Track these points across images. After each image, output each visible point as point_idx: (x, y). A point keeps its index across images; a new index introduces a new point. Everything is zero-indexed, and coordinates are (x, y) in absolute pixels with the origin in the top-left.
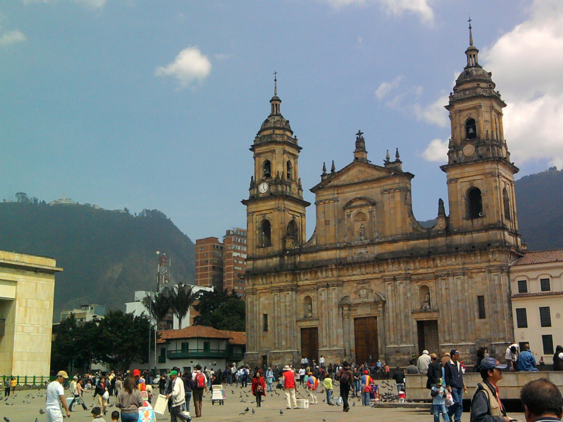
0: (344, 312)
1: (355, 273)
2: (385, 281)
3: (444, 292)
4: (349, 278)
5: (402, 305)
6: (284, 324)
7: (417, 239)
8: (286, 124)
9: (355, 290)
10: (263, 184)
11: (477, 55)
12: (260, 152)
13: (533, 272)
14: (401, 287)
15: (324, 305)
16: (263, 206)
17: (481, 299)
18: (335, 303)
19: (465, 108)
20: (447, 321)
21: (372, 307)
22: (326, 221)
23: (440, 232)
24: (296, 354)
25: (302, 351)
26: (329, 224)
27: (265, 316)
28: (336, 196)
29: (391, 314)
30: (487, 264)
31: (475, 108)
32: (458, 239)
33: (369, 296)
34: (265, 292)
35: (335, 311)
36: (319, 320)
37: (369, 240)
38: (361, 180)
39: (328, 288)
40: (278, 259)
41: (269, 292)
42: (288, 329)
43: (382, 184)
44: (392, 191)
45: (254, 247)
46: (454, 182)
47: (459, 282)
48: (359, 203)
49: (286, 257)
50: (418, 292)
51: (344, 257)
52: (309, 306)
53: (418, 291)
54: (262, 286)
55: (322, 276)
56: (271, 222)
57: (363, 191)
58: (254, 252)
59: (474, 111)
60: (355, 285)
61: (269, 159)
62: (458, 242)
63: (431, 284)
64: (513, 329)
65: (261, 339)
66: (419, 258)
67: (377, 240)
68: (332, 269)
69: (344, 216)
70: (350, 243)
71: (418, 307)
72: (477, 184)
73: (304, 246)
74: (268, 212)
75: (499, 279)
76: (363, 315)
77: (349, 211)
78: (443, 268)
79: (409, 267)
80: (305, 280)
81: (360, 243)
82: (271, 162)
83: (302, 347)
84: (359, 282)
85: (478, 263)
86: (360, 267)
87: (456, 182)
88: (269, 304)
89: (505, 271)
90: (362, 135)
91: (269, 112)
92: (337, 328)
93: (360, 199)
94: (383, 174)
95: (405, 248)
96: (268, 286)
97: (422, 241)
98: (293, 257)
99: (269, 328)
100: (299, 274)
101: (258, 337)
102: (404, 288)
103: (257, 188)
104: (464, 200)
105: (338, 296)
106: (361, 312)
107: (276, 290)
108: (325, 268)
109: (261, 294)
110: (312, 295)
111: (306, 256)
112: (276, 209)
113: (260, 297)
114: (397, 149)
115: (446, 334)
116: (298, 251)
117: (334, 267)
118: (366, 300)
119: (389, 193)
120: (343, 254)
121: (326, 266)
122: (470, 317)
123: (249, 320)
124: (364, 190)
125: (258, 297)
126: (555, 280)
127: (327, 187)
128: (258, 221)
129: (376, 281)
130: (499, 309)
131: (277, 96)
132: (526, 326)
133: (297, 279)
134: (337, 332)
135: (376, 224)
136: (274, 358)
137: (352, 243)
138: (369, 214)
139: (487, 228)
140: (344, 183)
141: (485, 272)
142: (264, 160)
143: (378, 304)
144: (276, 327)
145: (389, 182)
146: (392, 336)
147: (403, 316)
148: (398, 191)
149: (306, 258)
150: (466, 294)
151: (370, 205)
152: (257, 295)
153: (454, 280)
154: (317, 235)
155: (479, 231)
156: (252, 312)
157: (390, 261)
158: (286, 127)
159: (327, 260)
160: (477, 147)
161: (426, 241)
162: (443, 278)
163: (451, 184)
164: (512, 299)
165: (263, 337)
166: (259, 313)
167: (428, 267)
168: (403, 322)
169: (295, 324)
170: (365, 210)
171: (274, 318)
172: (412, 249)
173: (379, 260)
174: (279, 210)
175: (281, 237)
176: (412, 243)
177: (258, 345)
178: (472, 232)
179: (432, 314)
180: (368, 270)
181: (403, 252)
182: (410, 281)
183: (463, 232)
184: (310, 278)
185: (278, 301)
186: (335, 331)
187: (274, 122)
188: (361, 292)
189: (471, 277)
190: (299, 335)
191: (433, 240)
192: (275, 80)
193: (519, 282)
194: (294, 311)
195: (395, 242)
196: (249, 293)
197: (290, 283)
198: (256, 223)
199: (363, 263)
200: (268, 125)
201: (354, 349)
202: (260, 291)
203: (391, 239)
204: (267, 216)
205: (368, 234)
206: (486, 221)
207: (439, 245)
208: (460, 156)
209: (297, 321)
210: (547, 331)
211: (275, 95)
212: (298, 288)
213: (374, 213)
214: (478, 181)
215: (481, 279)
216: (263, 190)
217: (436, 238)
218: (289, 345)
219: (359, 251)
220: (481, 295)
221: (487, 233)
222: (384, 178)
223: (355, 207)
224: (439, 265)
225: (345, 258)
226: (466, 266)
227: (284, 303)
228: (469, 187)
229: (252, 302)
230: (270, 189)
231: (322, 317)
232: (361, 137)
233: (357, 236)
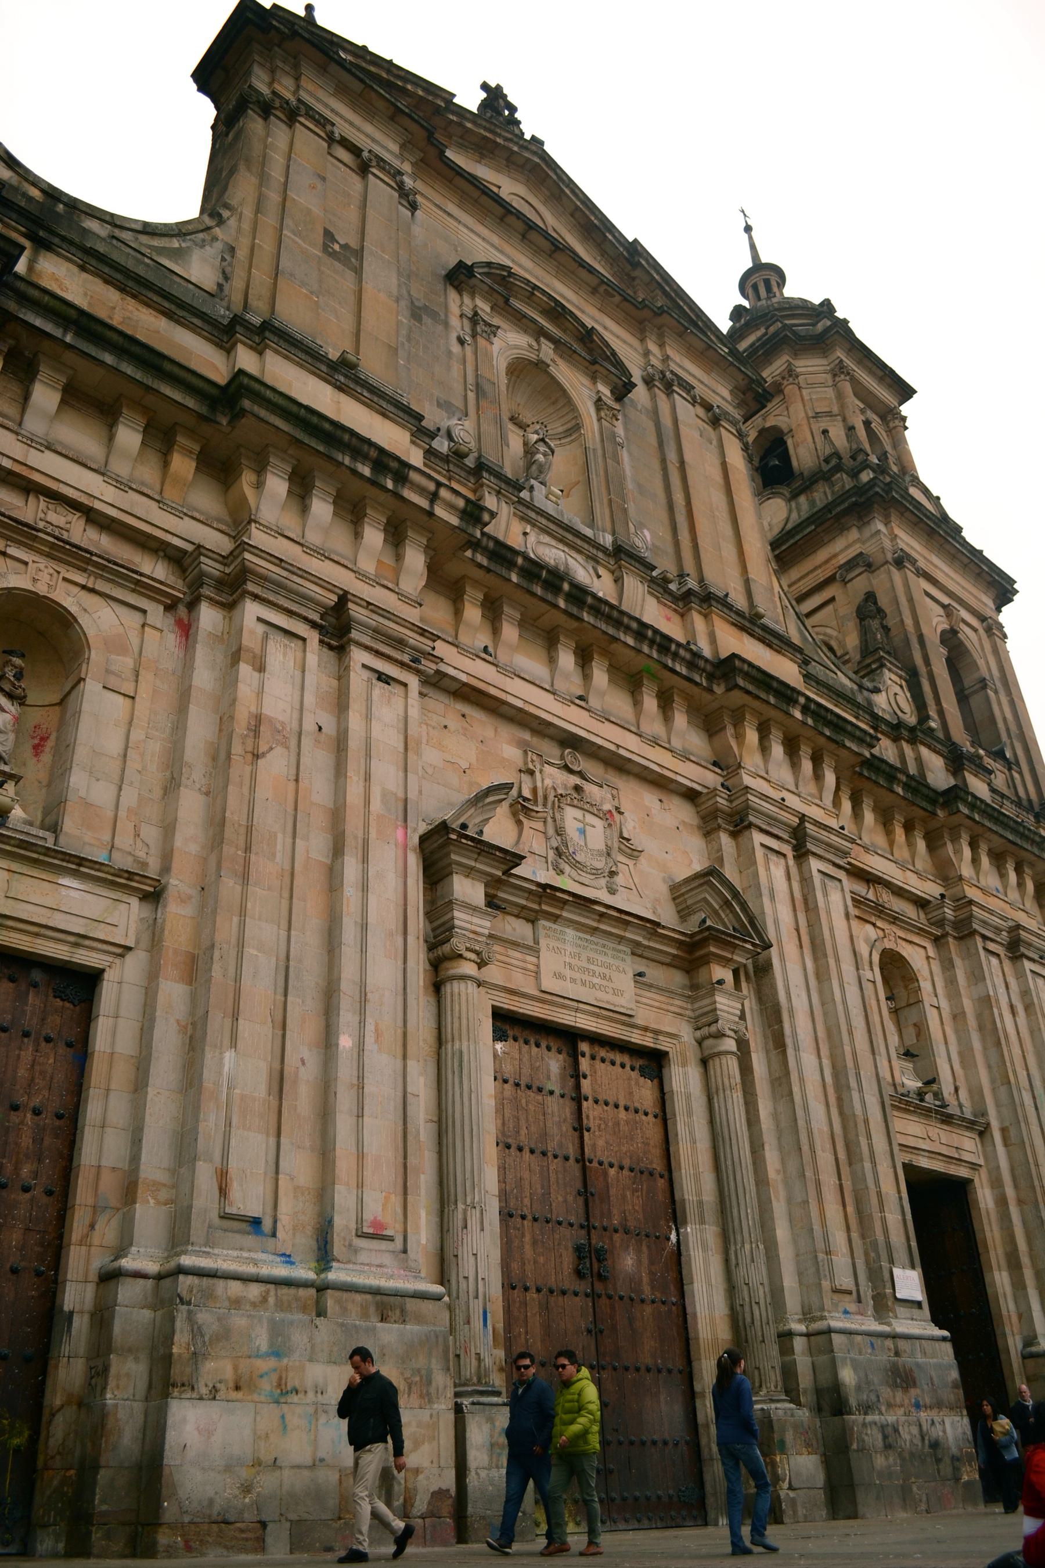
29: (809, 1060)
33: (619, 880)
60: (512, 753)
76: (577, 1004)
117: (454, 521)
129: (650, 798)
135: (630, 485)
162: (991, 946)
199: (628, 629)
217: (913, 741)
228: (946, 626)
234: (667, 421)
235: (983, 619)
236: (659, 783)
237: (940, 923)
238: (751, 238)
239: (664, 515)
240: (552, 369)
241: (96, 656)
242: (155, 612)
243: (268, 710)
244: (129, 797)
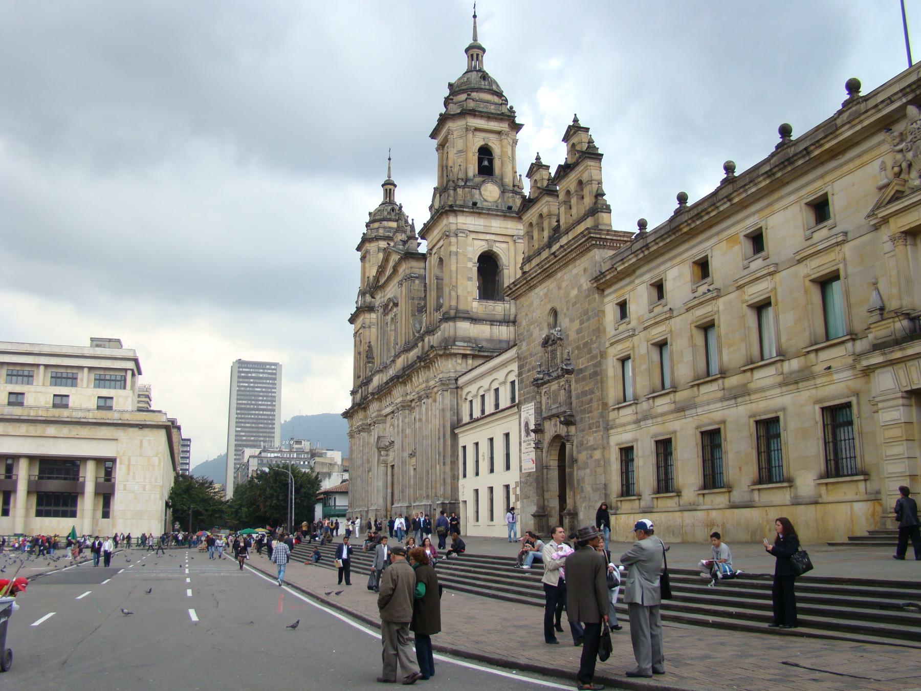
8: (389, 213)
11: (482, 56)
64: (458, 479)
72: (442, 254)
89: (452, 387)
104: (436, 281)
122: (432, 462)
158: (388, 217)
164: (456, 431)
192: (390, 159)
211: (389, 177)
238: (475, 23)
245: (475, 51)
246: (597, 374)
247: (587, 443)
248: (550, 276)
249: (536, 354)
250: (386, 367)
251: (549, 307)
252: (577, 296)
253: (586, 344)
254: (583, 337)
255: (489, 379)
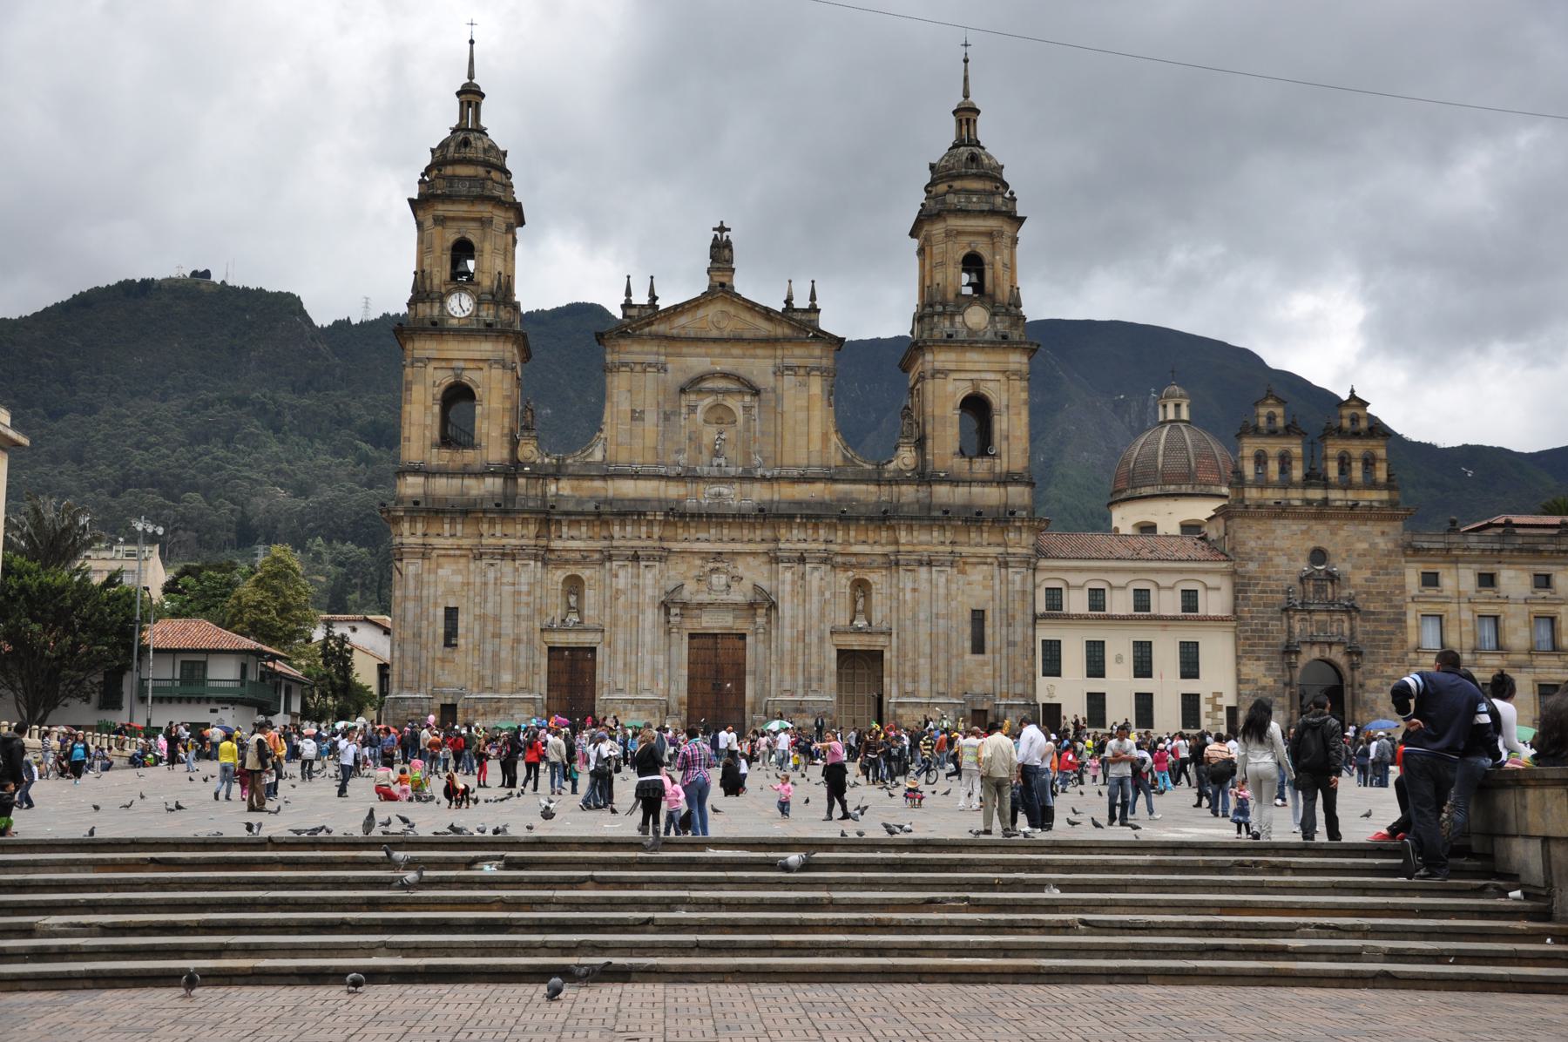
0: (672, 619)
1: (702, 535)
2: (775, 560)
3: (909, 596)
4: (685, 545)
5: (815, 614)
6: (508, 635)
7: (854, 481)
9: (696, 572)
10: (457, 295)
12: (451, 214)
13: (1078, 574)
14: (816, 577)
15: (622, 599)
16: (455, 350)
17: (978, 617)
18: (653, 597)
19: (969, 229)
20: (910, 655)
21: (737, 612)
22: (633, 411)
23: (909, 475)
24: (539, 705)
25: (548, 698)
26: (643, 420)
27: (451, 614)
28: (662, 358)
29: (787, 631)
30: (1001, 550)
31: (990, 234)
32: (942, 493)
33: (732, 589)
34: (454, 556)
35: (651, 616)
36: (603, 631)
37: (741, 469)
38: (725, 335)
39: (635, 563)
40: (499, 481)
41: (461, 556)
42: (522, 647)
43: (779, 352)
44: (802, 371)
45: (428, 443)
46: (943, 376)
47: (943, 579)
48: (721, 384)
49: (522, 481)
50: (848, 590)
51: (676, 497)
52: (572, 599)
53: (848, 588)
54: (451, 541)
55: (625, 536)
56: (478, 392)
57: (730, 360)
58: (427, 456)
59: (985, 239)
60: (698, 562)
61: (470, 236)
62: (944, 500)
63: (874, 577)
65: (438, 664)
66: (863, 522)
67: (759, 472)
68: (650, 523)
69: (680, 406)
70: (695, 470)
71: (843, 620)
73: (569, 461)
74: (471, 365)
75: (1024, 580)
76: (713, 628)
77: (693, 397)
78: (909, 548)
79: (832, 537)
80: (572, 540)
81: (715, 472)
82: (476, 245)
83: (548, 690)
84: (705, 556)
85: (982, 546)
86: (720, 525)
87: (946, 375)
88: (463, 584)
90: (726, 234)
91: (455, 121)
92: (654, 652)
93: (725, 376)
94: (782, 331)
95: (827, 497)
96: (466, 542)
97: (863, 487)
98: (541, 481)
99: (461, 641)
100: (559, 522)
101: (430, 660)
102: (822, 579)
103: (442, 303)
105: (657, 581)
106: (711, 622)
107: (493, 553)
108: (636, 517)
109: (441, 560)
110: (586, 573)
111: (575, 483)
112: (496, 362)
113: (439, 566)
114: (813, 282)
115: (908, 679)
116: (551, 470)
117: (662, 518)
118: (724, 597)
119: (796, 375)
120: (673, 491)
121: (639, 514)
123: (410, 616)
124: (733, 357)
125: (433, 566)
126: (1116, 593)
127: (650, 334)
128: (440, 384)
129: (750, 559)
130: (1019, 638)
131: (474, 81)
132: (1059, 674)
133: (549, 532)
134: (653, 663)
136: (481, 711)
137: (698, 468)
138: (741, 413)
139: (1006, 480)
140: (683, 333)
141: (992, 564)
142: (457, 236)
143: (755, 609)
144: (489, 639)
145: (798, 351)
146: (787, 677)
147: (815, 640)
148: (818, 373)
149: (572, 488)
150: (954, 604)
151: (747, 393)
152: (432, 561)
153: (931, 572)
154: (606, 439)
155: (984, 482)
156: (419, 599)
157: (798, 520)
159: (635, 500)
160: (994, 315)
161: (872, 488)
162: (909, 568)
163: (936, 380)
165: (443, 660)
166: (436, 604)
167: (875, 542)
168: (814, 650)
169: (538, 635)
170: (734, 403)
171: (483, 618)
172: (839, 500)
173: (766, 516)
174: (504, 367)
175: (506, 431)
176: (841, 487)
177: (429, 682)
178: (971, 482)
179: (874, 638)
180: (736, 533)
181: (822, 504)
182: (833, 567)
183: (954, 481)
184: (584, 536)
185: (496, 579)
186: (648, 658)
187: (485, 151)
188: (715, 578)
189: (960, 572)
190: (545, 661)
191: (887, 487)
192: (472, 42)
193: (1047, 589)
194: (538, 606)
195: (804, 482)
196: (415, 553)
197: (533, 542)
198: (434, 386)
200: (469, 153)
201: (686, 701)
202: (443, 552)
203: (795, 473)
204: (466, 373)
205: (730, 452)
206: (1001, 466)
207: (903, 499)
208: (958, 325)
209: (542, 630)
210: (1096, 685)
211: (471, 76)
212: (548, 556)
213: (755, 411)
214: (990, 385)
215: (981, 578)
216: (459, 310)
218: (522, 683)
219: (716, 489)
220: (979, 608)
221: (1002, 490)
222: (788, 340)
223: (712, 391)
224: (903, 540)
225: (678, 501)
226: (957, 549)
227: (514, 584)
228: (970, 391)
229: (418, 577)
230: (478, 310)
231: (614, 624)
232: (725, 238)
233: (705, 457)
234: (779, 391)
235: (1005, 371)
236: (754, 554)
237: (891, 561)
238: (966, 70)
239: (772, 440)
240: (725, 403)
241: (586, 583)
242: (597, 567)
243: (620, 587)
244: (597, 612)
245: (966, 115)
246: (1399, 620)
247: (1382, 672)
248: (1315, 518)
249: (1278, 580)
250: (695, 478)
251: (1311, 545)
252: (1364, 550)
253: (1379, 593)
254: (1379, 587)
255: (1132, 577)
